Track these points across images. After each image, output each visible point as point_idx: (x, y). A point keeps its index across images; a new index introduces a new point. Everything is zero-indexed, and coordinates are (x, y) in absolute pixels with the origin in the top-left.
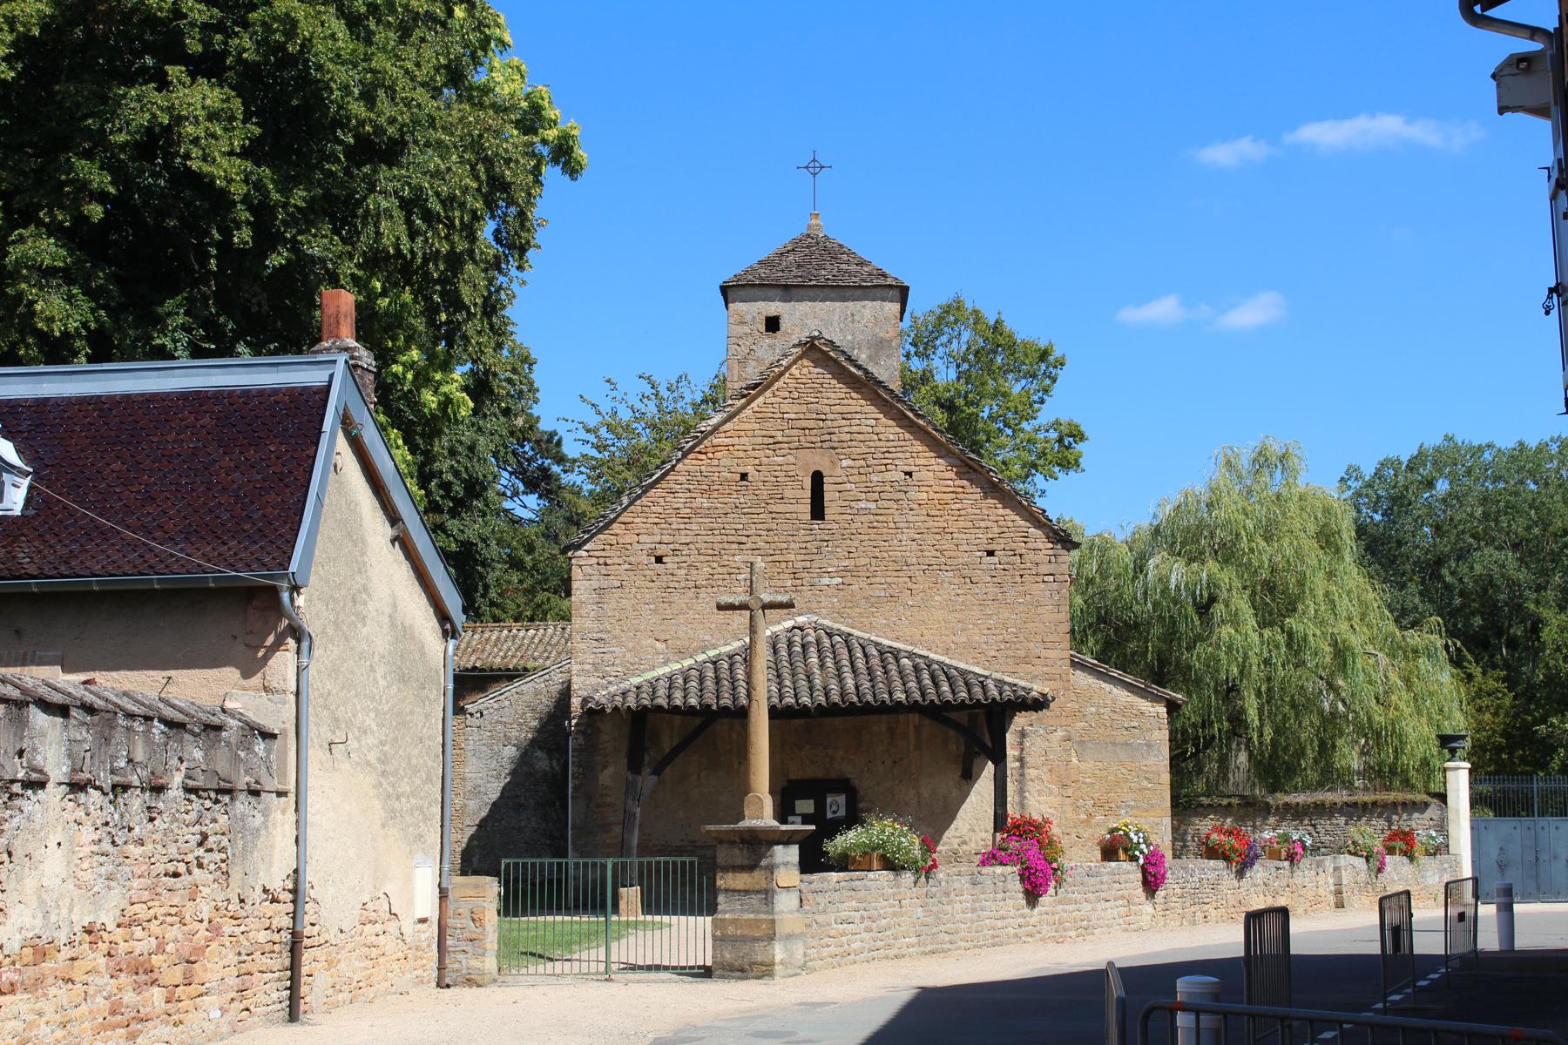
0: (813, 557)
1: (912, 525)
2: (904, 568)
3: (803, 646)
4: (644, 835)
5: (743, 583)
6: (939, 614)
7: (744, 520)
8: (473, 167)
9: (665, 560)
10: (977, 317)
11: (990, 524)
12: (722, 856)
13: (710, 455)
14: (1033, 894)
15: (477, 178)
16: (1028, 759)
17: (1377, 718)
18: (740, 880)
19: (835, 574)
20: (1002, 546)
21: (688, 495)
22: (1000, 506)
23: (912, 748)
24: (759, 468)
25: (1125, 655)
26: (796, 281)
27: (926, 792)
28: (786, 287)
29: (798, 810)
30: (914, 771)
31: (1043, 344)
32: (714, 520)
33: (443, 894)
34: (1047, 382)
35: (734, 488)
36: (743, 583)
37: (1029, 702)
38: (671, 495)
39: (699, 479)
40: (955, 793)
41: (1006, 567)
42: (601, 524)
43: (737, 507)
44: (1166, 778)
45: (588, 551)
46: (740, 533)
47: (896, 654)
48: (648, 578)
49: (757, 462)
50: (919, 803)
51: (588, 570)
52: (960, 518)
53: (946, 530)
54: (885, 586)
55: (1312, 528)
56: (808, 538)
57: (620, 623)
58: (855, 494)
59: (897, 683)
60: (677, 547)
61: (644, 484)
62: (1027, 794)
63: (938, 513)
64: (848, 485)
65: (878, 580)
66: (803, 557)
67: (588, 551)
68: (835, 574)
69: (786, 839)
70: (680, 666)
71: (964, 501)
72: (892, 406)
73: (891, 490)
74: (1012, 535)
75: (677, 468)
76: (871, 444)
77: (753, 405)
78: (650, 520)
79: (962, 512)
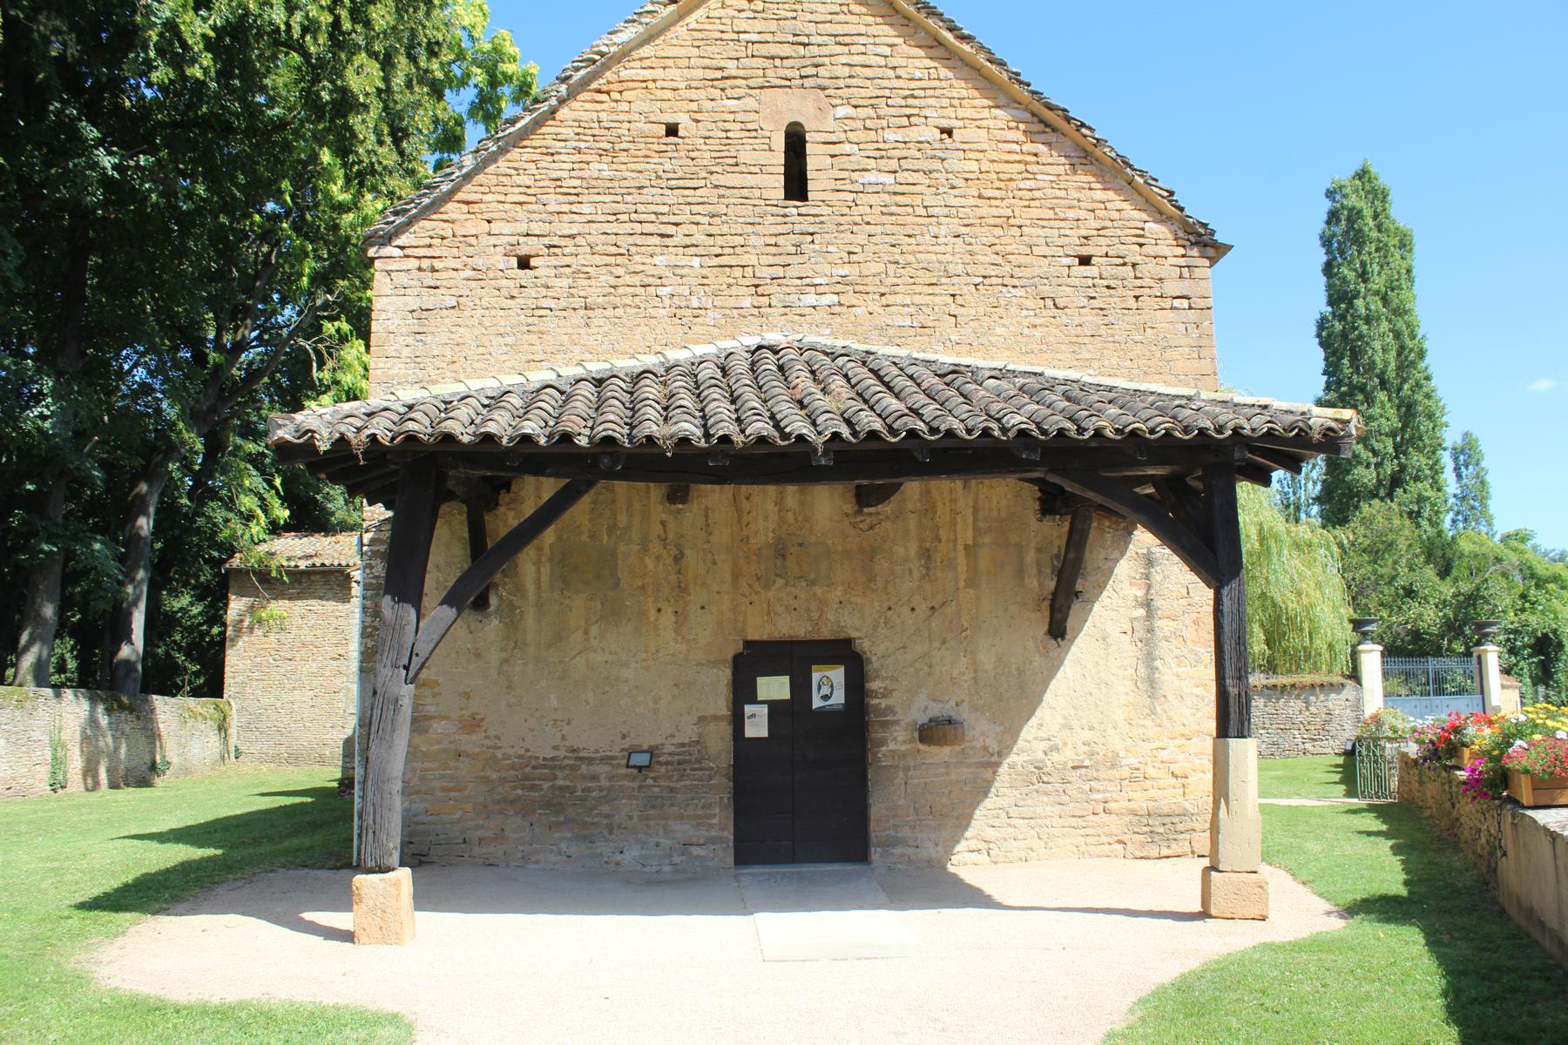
0: (788, 259)
1: (954, 211)
2: (944, 280)
3: (781, 368)
4: (488, 737)
5: (667, 302)
7: (671, 197)
9: (533, 262)
11: (1082, 214)
13: (616, 96)
16: (1158, 603)
17: (1290, 605)
19: (826, 289)
20: (1104, 250)
21: (577, 157)
22: (1099, 186)
23: (962, 584)
24: (698, 116)
27: (987, 661)
29: (762, 695)
30: (966, 625)
32: (619, 198)
35: (656, 147)
36: (667, 302)
37: (1316, 436)
38: (549, 158)
39: (596, 132)
40: (1038, 661)
41: (1112, 283)
42: (426, 201)
43: (659, 177)
45: (402, 248)
46: (665, 218)
48: (504, 292)
49: (694, 106)
50: (975, 680)
51: (402, 279)
52: (1033, 203)
53: (1012, 221)
54: (912, 310)
56: (780, 229)
57: (454, 367)
58: (858, 160)
60: (556, 241)
61: (501, 134)
62: (1158, 663)
63: (997, 193)
64: (847, 148)
65: (898, 299)
66: (772, 260)
67: (402, 248)
68: (826, 289)
70: (522, 380)
71: (1039, 177)
72: (918, 26)
73: (919, 155)
74: (1119, 233)
75: (559, 115)
76: (885, 83)
77: (688, 20)
78: (511, 198)
79: (1037, 194)
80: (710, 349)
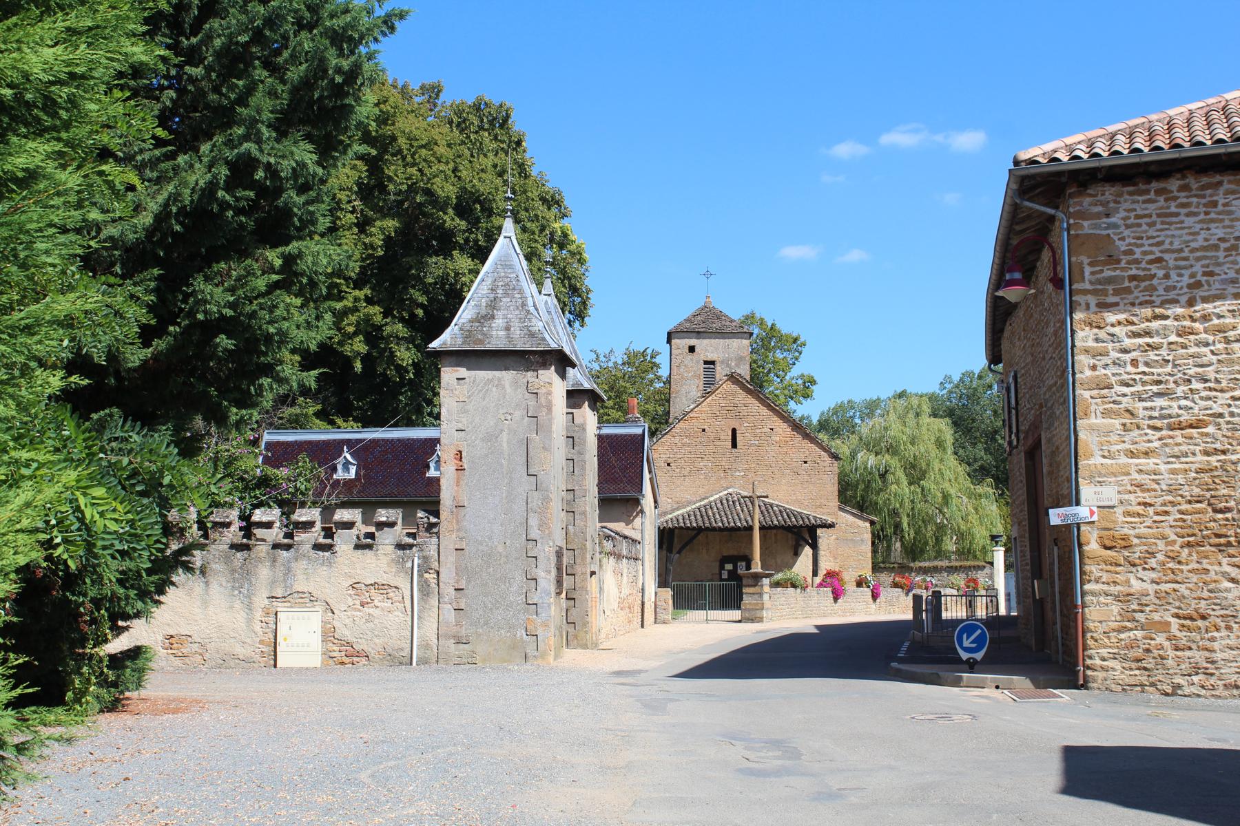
6: (784, 488)
8: (562, 282)
10: (762, 322)
12: (744, 582)
14: (836, 599)
15: (564, 286)
18: (751, 590)
25: (846, 497)
26: (702, 330)
27: (779, 561)
28: (698, 332)
31: (795, 335)
33: (656, 593)
34: (797, 354)
44: (870, 555)
47: (771, 505)
55: (933, 439)
59: (774, 518)
69: (767, 576)
80: (717, 496)
